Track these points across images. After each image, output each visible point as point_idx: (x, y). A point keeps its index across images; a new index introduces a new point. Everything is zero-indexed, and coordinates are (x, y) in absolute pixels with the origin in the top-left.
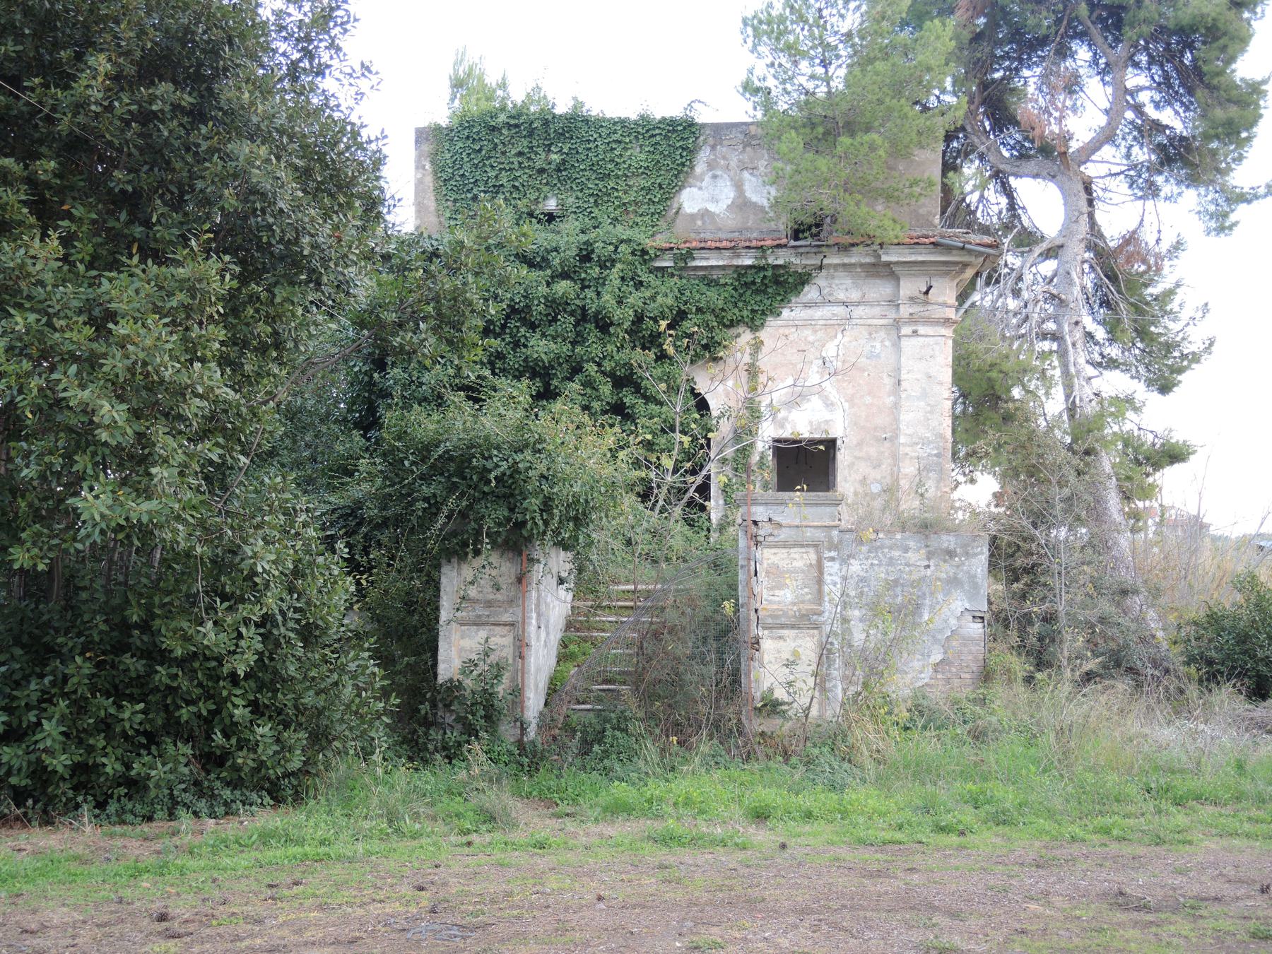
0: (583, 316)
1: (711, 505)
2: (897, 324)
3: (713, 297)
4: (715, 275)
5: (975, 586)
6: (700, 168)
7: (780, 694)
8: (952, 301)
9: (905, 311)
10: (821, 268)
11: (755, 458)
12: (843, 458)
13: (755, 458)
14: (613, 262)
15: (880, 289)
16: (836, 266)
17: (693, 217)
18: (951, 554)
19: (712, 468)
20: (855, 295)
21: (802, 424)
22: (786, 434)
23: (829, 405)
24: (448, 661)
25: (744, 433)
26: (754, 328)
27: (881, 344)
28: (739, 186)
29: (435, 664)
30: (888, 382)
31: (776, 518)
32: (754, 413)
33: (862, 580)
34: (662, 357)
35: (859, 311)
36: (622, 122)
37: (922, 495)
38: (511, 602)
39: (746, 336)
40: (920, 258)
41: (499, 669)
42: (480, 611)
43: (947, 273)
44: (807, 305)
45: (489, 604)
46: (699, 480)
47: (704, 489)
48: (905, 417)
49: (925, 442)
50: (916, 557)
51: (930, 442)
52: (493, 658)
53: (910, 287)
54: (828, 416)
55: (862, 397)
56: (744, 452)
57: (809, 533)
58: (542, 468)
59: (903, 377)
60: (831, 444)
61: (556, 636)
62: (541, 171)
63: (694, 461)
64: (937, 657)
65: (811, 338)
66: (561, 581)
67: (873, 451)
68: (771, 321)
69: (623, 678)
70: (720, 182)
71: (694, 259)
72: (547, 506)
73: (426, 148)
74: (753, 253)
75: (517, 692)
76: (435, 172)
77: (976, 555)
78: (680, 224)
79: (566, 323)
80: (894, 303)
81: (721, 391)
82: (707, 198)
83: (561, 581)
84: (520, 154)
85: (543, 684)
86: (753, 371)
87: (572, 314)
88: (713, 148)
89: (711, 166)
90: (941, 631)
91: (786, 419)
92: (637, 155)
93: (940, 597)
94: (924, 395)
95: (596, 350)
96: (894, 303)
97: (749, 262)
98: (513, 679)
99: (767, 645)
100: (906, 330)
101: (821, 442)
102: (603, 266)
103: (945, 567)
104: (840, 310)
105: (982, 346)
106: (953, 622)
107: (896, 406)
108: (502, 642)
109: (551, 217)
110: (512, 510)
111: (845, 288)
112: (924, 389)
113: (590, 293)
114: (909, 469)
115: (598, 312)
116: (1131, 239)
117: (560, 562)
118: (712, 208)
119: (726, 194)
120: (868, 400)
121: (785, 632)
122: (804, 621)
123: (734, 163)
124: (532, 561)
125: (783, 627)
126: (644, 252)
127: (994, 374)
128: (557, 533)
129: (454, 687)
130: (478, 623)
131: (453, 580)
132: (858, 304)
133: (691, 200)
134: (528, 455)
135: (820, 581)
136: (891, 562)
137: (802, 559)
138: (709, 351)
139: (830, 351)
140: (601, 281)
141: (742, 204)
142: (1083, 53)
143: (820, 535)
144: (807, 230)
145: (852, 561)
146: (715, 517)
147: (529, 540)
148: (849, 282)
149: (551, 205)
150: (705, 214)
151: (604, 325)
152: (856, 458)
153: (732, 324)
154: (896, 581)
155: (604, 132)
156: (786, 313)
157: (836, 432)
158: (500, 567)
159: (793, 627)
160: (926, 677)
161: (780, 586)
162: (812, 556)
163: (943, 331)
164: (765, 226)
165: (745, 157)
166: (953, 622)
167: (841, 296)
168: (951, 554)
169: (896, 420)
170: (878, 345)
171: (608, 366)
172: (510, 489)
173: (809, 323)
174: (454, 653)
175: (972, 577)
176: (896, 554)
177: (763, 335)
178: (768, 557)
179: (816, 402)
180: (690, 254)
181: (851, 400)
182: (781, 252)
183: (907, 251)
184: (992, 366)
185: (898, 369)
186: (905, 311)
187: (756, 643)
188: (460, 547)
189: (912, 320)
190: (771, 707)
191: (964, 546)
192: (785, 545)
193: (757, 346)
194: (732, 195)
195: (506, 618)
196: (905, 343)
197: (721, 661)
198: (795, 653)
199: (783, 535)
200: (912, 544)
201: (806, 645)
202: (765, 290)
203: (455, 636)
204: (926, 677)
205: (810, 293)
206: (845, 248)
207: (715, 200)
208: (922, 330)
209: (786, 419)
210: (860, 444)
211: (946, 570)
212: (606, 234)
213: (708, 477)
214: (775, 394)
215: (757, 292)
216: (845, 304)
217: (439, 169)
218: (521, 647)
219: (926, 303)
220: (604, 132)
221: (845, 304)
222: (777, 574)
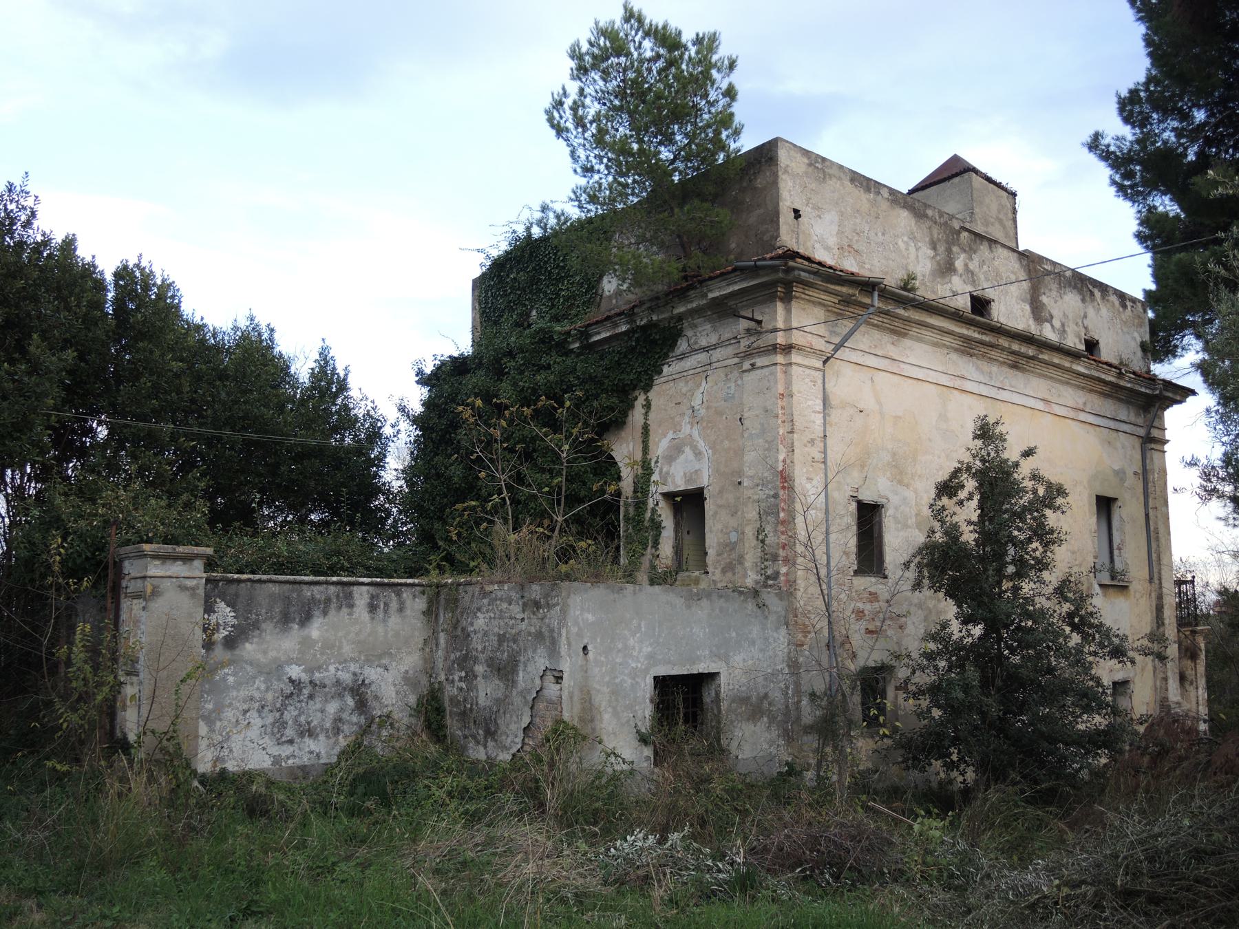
17: (610, 297)
20: (713, 339)
23: (698, 454)
35: (717, 354)
37: (763, 542)
40: (736, 287)
43: (772, 298)
44: (683, 356)
49: (764, 483)
50: (516, 609)
51: (769, 482)
54: (697, 467)
55: (722, 442)
59: (746, 415)
65: (684, 390)
68: (658, 380)
71: (591, 336)
74: (623, 319)
77: (554, 605)
78: (604, 305)
86: (646, 430)
90: (529, 691)
91: (668, 473)
97: (624, 328)
104: (702, 357)
111: (705, 334)
112: (762, 425)
114: (752, 514)
120: (726, 444)
132: (715, 347)
139: (696, 402)
145: (479, 614)
148: (708, 327)
152: (720, 506)
154: (504, 635)
156: (666, 369)
157: (704, 481)
170: (733, 385)
173: (682, 374)
177: (651, 395)
181: (713, 447)
183: (723, 283)
193: (648, 406)
205: (682, 346)
208: (760, 362)
209: (668, 473)
210: (721, 492)
214: (660, 446)
221: (706, 349)
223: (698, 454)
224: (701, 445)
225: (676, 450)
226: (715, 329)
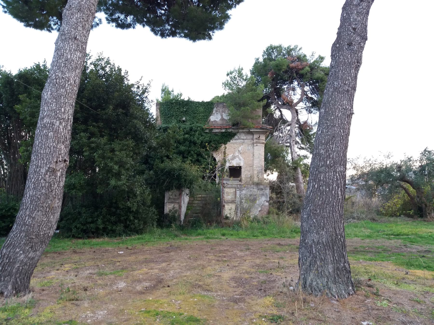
0: (190, 142)
1: (216, 179)
2: (253, 144)
3: (216, 138)
4: (217, 133)
5: (267, 196)
6: (214, 112)
7: (228, 215)
8: (264, 139)
9: (255, 141)
10: (238, 132)
11: (225, 170)
12: (243, 170)
13: (225, 170)
14: (197, 131)
15: (250, 137)
16: (241, 132)
17: (213, 122)
18: (262, 189)
19: (217, 172)
20: (245, 138)
21: (234, 163)
22: (231, 165)
23: (240, 159)
24: (166, 210)
25: (223, 165)
26: (225, 144)
27: (250, 147)
28: (222, 116)
29: (164, 210)
30: (252, 155)
31: (228, 183)
32: (225, 162)
33: (245, 194)
34: (206, 150)
35: (246, 141)
36: (198, 102)
38: (178, 199)
39: (223, 146)
41: (176, 211)
42: (173, 200)
43: (263, 134)
44: (236, 140)
45: (174, 199)
46: (214, 175)
47: (215, 177)
48: (255, 162)
49: (259, 167)
50: (255, 190)
52: (175, 209)
53: (256, 136)
56: (223, 169)
57: (234, 186)
58: (184, 174)
60: (240, 167)
61: (186, 205)
62: (182, 112)
63: (213, 171)
64: (260, 209)
66: (187, 195)
67: (249, 169)
68: (228, 143)
69: (199, 213)
70: (218, 115)
72: (185, 181)
73: (158, 107)
75: (179, 215)
76: (160, 112)
79: (187, 143)
80: (253, 139)
81: (218, 157)
82: (216, 118)
83: (187, 195)
84: (178, 108)
85: (184, 214)
86: (225, 153)
87: (188, 141)
88: (217, 108)
89: (216, 111)
92: (201, 109)
93: (260, 198)
94: (259, 158)
95: (194, 149)
96: (253, 139)
98: (179, 213)
99: (226, 206)
100: (255, 145)
101: (238, 167)
102: (195, 132)
103: (261, 192)
104: (242, 141)
105: (274, 146)
106: (263, 202)
107: (253, 160)
108: (177, 206)
109: (184, 121)
110: (179, 181)
111: (243, 136)
113: (192, 137)
114: (256, 172)
115: (194, 141)
116: (306, 122)
117: (187, 191)
118: (216, 120)
119: (219, 117)
121: (229, 204)
122: (233, 202)
123: (221, 111)
124: (182, 191)
125: (229, 203)
126: (203, 129)
127: (276, 151)
128: (187, 186)
129: (167, 215)
130: (172, 203)
131: (167, 195)
132: (246, 139)
133: (212, 118)
134: (182, 171)
135: (236, 195)
136: (251, 191)
137: (232, 190)
138: (216, 149)
139: (240, 149)
140: (194, 135)
141: (222, 119)
142: (296, 83)
143: (236, 186)
144: (236, 124)
146: (217, 182)
147: (182, 187)
149: (184, 119)
150: (215, 121)
151: (195, 143)
153: (221, 143)
155: (195, 104)
156: (231, 141)
157: (242, 165)
158: (177, 192)
159: (231, 203)
160: (257, 213)
161: (229, 195)
162: (234, 190)
163: (262, 145)
164: (227, 124)
165: (223, 110)
166: (263, 202)
167: (242, 138)
168: (262, 189)
169: (253, 163)
171: (196, 152)
172: (179, 177)
173: (236, 143)
174: (167, 208)
175: (266, 194)
176: (252, 189)
177: (226, 146)
178: (226, 190)
179: (237, 159)
180: (212, 129)
181: (244, 159)
182: (230, 129)
184: (276, 150)
185: (254, 153)
186: (255, 141)
187: (224, 206)
188: (169, 189)
189: (256, 143)
190: (227, 218)
191: (265, 188)
192: (229, 188)
193: (226, 148)
194: (221, 117)
195: (177, 202)
196: (255, 147)
197: (217, 210)
198: (231, 208)
199: (229, 186)
200: (255, 187)
201: (233, 206)
202: (227, 137)
203: (168, 205)
204: (257, 213)
205: (236, 137)
206: (243, 129)
207: (217, 118)
208: (258, 145)
210: (246, 167)
211: (261, 192)
212: (195, 125)
213: (216, 174)
214: (230, 157)
215: (226, 137)
216: (243, 139)
217: (161, 111)
218: (180, 207)
219: (259, 139)
220: (195, 104)
221: (243, 139)
222: (228, 193)
223: (240, 159)
224: (241, 158)
225: (234, 158)
226: (245, 136)
